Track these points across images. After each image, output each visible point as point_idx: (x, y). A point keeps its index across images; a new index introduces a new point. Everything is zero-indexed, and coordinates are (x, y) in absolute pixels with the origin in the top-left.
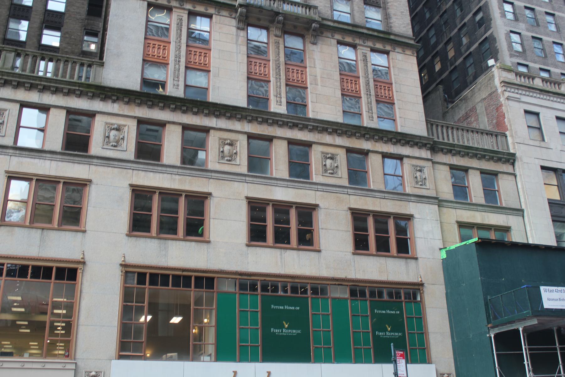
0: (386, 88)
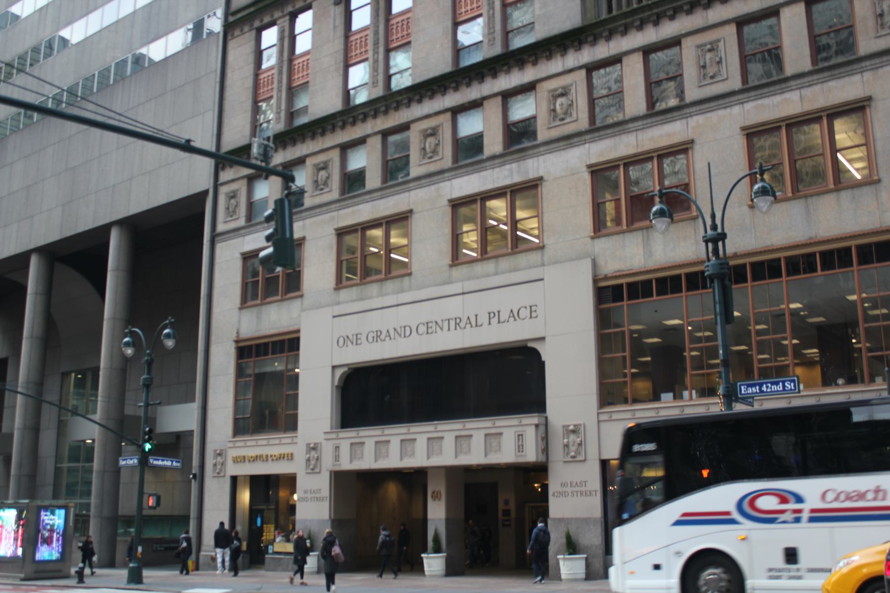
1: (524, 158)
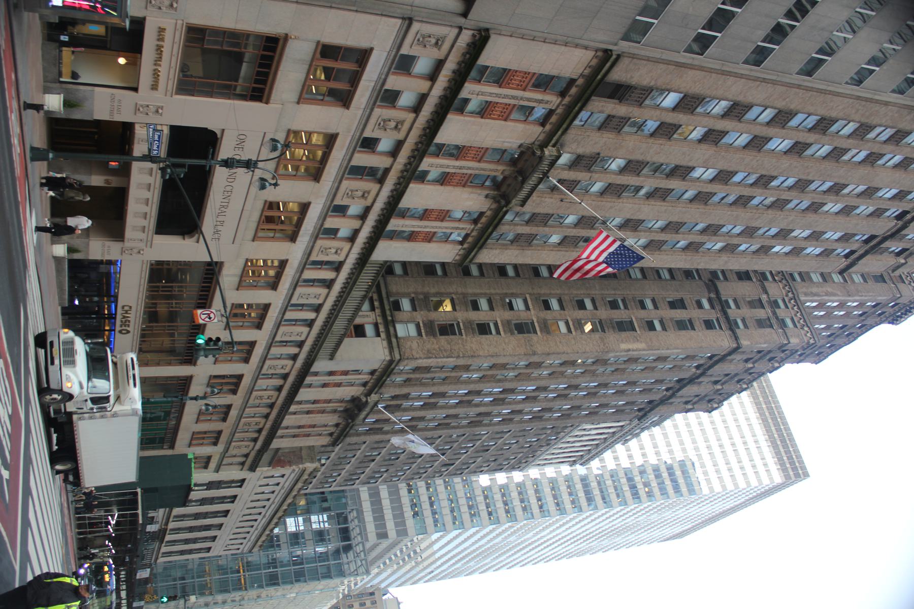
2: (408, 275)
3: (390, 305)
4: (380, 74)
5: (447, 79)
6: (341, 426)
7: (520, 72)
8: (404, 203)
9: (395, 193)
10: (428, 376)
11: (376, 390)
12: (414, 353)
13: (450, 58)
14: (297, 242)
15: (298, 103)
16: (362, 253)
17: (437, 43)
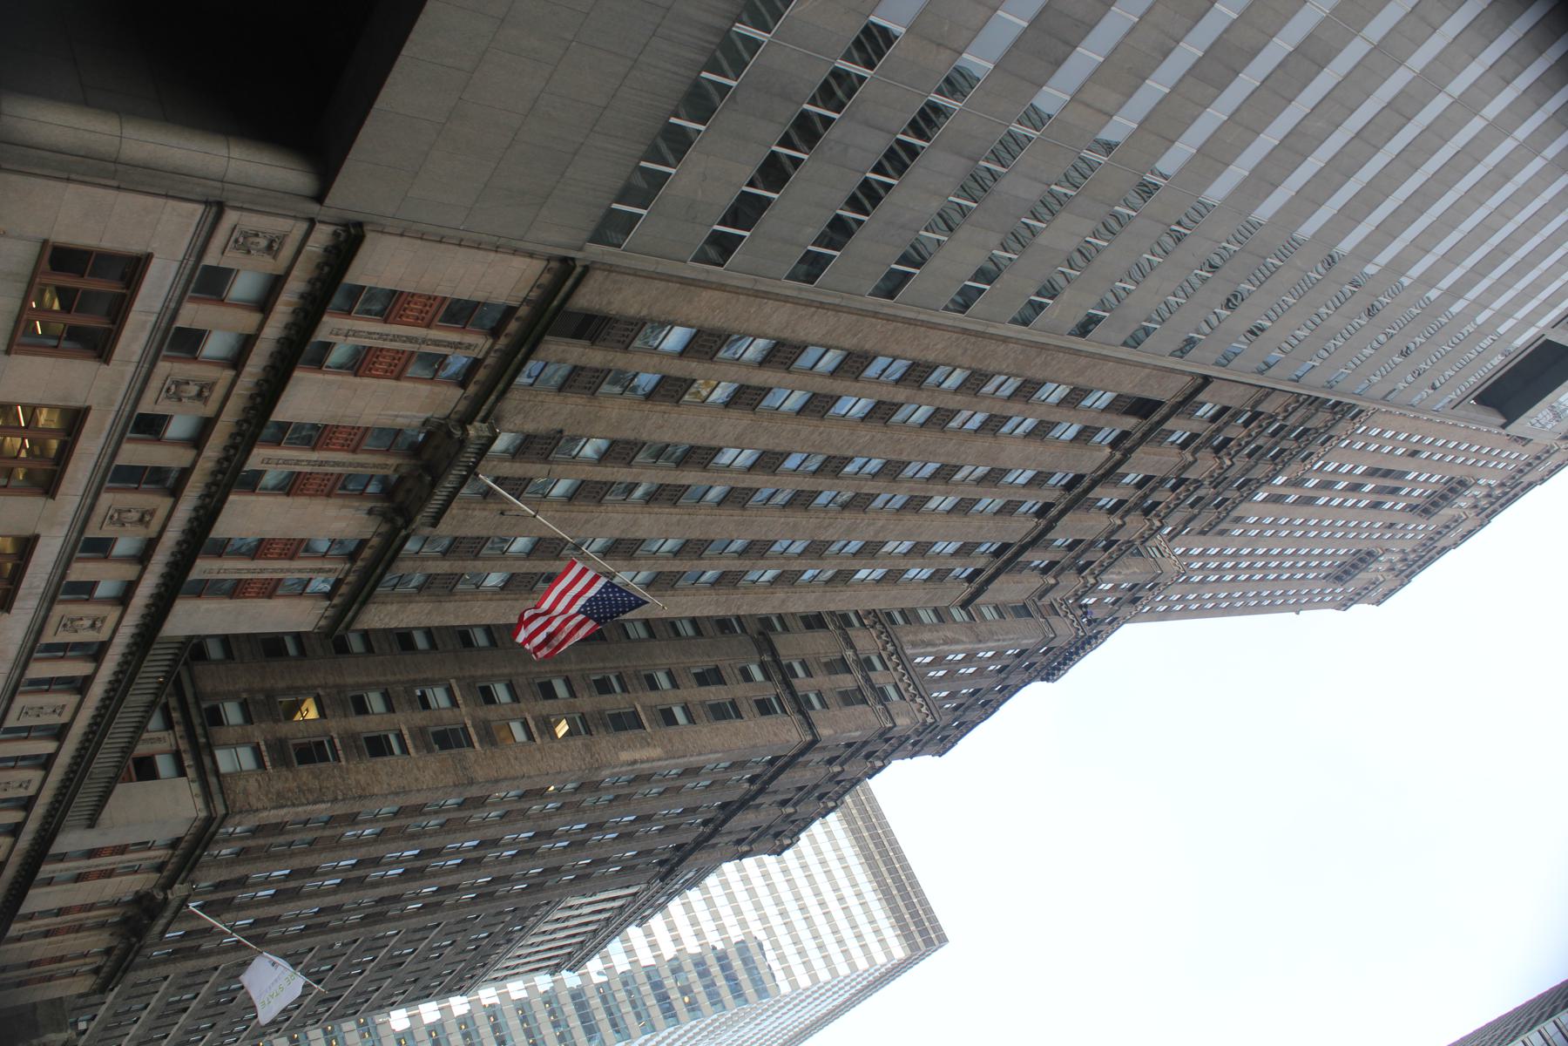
0: (423, 315)
1: (42, 599)
2: (233, 659)
3: (201, 717)
4: (167, 300)
5: (291, 309)
6: (116, 952)
7: (420, 296)
8: (221, 530)
9: (201, 512)
10: (281, 839)
11: (183, 875)
12: (253, 801)
13: (295, 272)
14: (13, 611)
15: (8, 352)
16: (144, 624)
17: (269, 247)
